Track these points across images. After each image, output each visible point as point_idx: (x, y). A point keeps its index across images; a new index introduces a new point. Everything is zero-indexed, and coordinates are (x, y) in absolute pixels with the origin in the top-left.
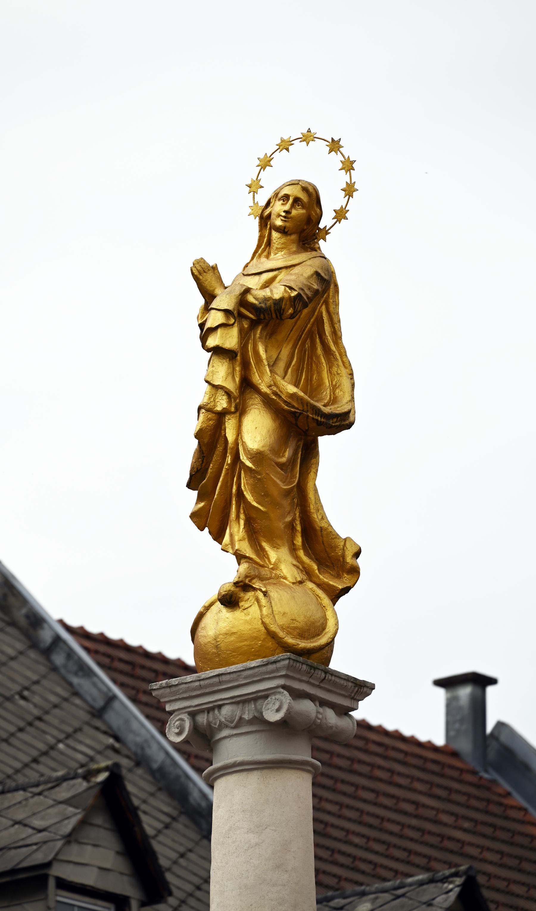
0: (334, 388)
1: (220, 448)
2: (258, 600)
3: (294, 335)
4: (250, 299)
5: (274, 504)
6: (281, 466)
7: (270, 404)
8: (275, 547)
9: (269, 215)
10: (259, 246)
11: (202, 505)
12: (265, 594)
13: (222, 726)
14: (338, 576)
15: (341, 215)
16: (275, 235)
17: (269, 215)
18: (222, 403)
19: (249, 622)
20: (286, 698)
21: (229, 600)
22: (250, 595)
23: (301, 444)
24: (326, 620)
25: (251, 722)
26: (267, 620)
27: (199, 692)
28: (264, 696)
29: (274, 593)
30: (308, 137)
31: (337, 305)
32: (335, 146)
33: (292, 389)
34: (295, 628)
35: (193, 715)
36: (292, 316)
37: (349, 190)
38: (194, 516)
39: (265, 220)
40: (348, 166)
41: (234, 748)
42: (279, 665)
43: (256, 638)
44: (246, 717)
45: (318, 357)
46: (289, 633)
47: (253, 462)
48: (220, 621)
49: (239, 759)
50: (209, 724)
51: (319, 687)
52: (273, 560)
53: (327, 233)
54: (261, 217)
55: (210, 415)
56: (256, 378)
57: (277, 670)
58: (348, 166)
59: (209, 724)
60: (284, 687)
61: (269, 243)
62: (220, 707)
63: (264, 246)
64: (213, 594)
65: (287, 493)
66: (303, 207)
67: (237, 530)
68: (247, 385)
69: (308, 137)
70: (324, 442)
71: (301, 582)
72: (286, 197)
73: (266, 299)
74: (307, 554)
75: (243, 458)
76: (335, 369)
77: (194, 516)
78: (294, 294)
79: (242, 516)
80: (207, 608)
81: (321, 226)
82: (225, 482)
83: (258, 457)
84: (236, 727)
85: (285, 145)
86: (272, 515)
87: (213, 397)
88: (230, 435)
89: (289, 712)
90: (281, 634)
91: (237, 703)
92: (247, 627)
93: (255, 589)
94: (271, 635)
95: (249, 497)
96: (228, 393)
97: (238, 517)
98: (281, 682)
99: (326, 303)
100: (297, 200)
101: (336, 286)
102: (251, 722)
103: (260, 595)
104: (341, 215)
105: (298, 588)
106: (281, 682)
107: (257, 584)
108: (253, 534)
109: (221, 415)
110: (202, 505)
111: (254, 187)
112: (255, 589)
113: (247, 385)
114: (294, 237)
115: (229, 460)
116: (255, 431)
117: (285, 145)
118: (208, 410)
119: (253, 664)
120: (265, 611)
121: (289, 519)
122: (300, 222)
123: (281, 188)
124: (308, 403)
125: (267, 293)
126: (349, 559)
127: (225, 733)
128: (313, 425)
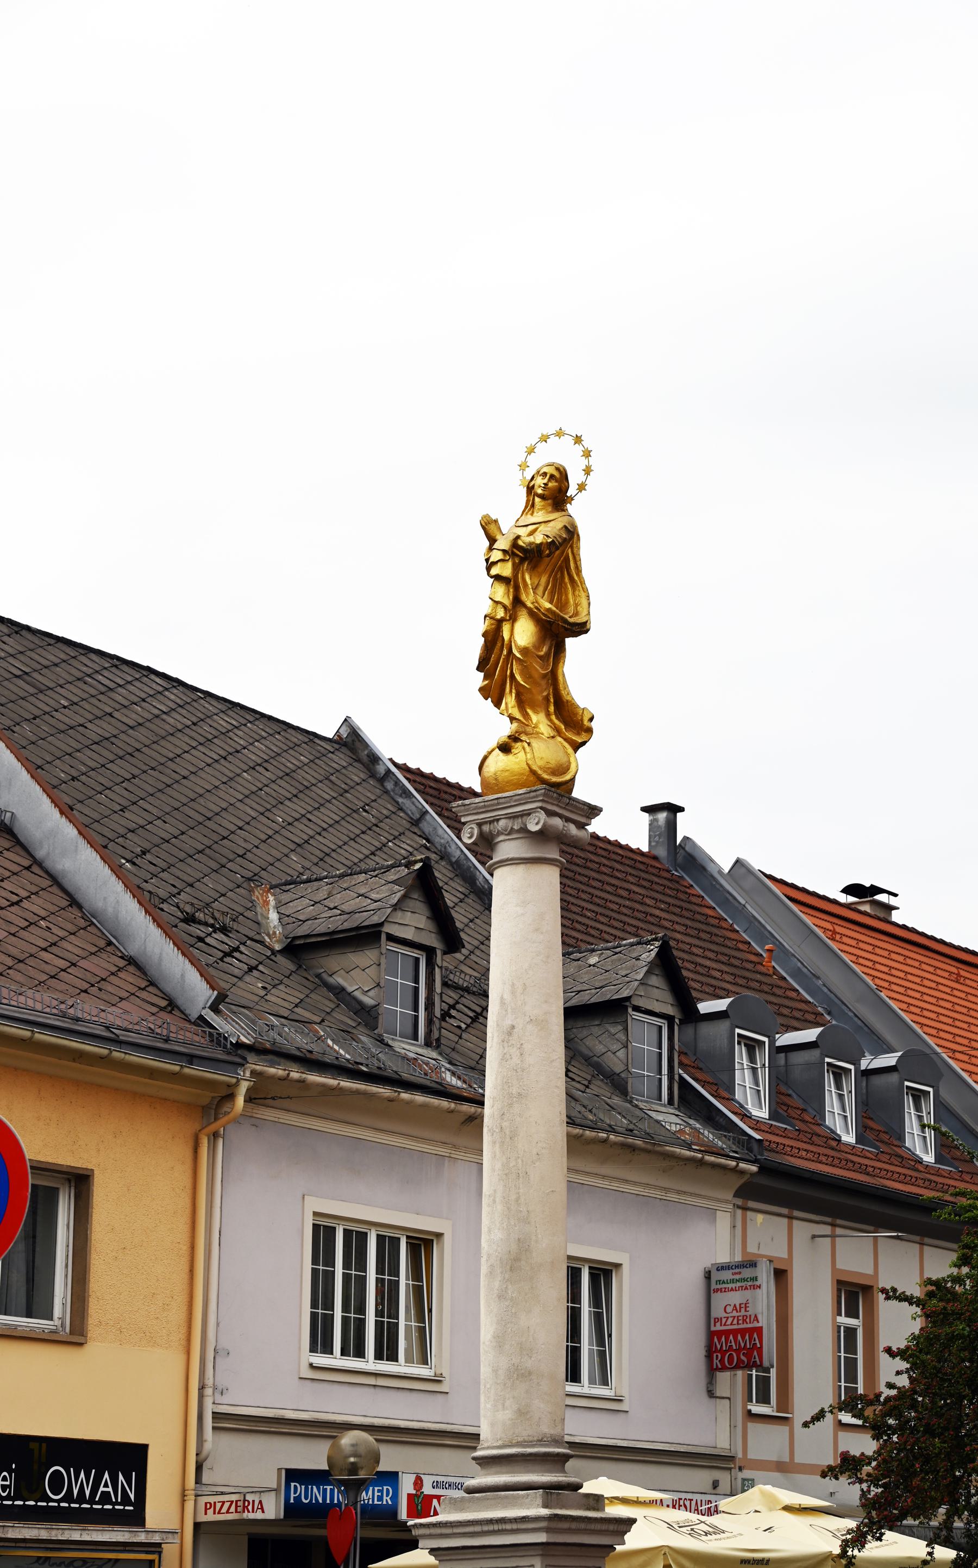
0: (576, 605)
1: (499, 644)
2: (524, 748)
3: (549, 568)
4: (520, 543)
5: (535, 683)
6: (540, 657)
7: (533, 614)
8: (536, 712)
9: (533, 486)
10: (526, 507)
11: (486, 682)
12: (529, 744)
13: (499, 833)
14: (578, 734)
15: (582, 487)
16: (537, 500)
17: (533, 486)
18: (500, 613)
19: (518, 763)
20: (542, 815)
21: (505, 748)
22: (519, 744)
23: (554, 643)
24: (570, 763)
25: (518, 831)
26: (530, 762)
28: (528, 813)
29: (535, 744)
30: (560, 433)
31: (579, 549)
32: (578, 440)
33: (548, 605)
34: (549, 768)
35: (480, 825)
36: (548, 556)
37: (588, 471)
38: (481, 690)
39: (530, 489)
40: (587, 454)
41: (507, 849)
42: (538, 793)
43: (522, 774)
44: (516, 827)
45: (566, 584)
46: (545, 771)
47: (521, 655)
48: (499, 762)
49: (511, 856)
50: (490, 831)
51: (564, 808)
52: (534, 721)
53: (572, 499)
54: (528, 487)
55: (493, 622)
56: (523, 597)
57: (537, 796)
58: (587, 454)
59: (490, 831)
60: (541, 808)
61: (533, 505)
62: (498, 820)
63: (530, 507)
64: (494, 744)
65: (544, 676)
66: (556, 481)
67: (510, 700)
68: (517, 602)
69: (560, 433)
70: (569, 642)
71: (553, 737)
72: (545, 474)
73: (531, 544)
74: (557, 718)
75: (515, 651)
76: (577, 593)
77: (481, 690)
78: (550, 540)
79: (514, 691)
80: (490, 753)
81: (568, 494)
82: (502, 668)
83: (524, 651)
84: (509, 834)
85: (544, 439)
86: (534, 691)
87: (494, 609)
88: (506, 635)
89: (544, 825)
90: (540, 772)
91: (510, 818)
92: (517, 767)
93: (522, 741)
94: (533, 772)
95: (518, 677)
96: (505, 607)
97: (511, 691)
98: (539, 804)
99: (572, 547)
100: (552, 476)
101: (578, 535)
102: (518, 831)
103: (526, 745)
104: (582, 487)
105: (551, 741)
106: (539, 804)
107: (523, 737)
108: (521, 703)
109: (500, 622)
110: (486, 682)
111: (523, 466)
112: (522, 741)
113: (517, 602)
114: (550, 501)
115: (505, 652)
116: (523, 633)
117: (544, 439)
118: (491, 618)
119: (521, 791)
120: (529, 756)
121: (545, 694)
122: (555, 492)
123: (541, 468)
124: (559, 615)
125: (531, 539)
126: (586, 722)
127: (501, 838)
128: (562, 630)
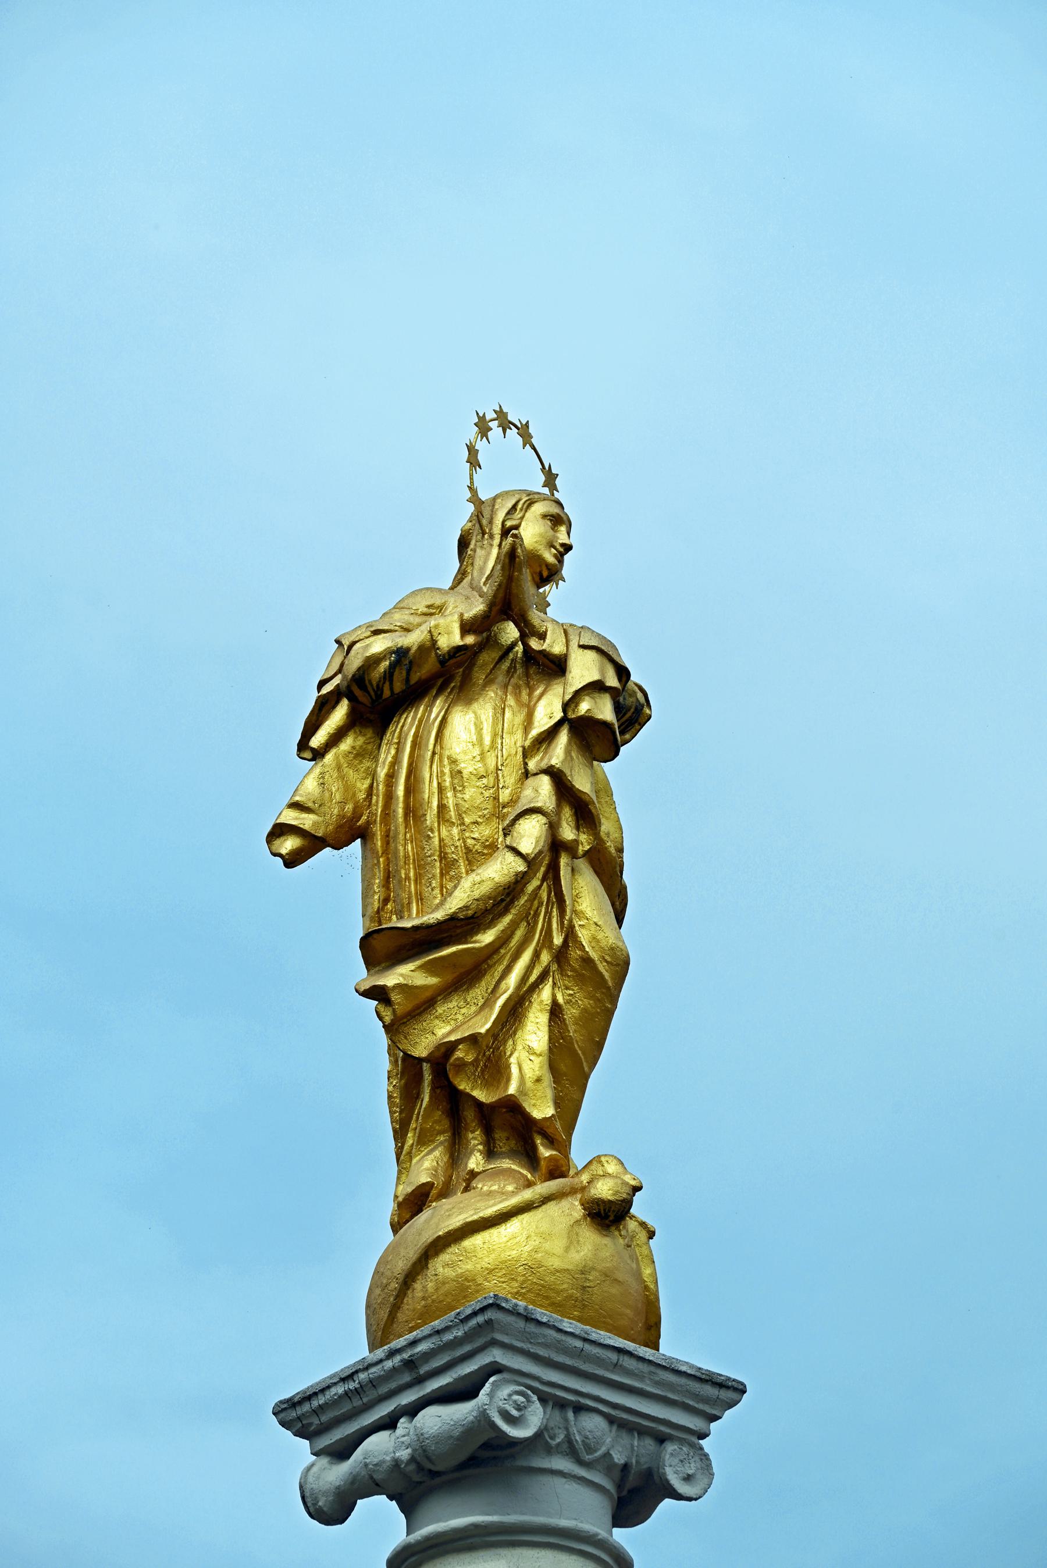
27: (568, 1361)
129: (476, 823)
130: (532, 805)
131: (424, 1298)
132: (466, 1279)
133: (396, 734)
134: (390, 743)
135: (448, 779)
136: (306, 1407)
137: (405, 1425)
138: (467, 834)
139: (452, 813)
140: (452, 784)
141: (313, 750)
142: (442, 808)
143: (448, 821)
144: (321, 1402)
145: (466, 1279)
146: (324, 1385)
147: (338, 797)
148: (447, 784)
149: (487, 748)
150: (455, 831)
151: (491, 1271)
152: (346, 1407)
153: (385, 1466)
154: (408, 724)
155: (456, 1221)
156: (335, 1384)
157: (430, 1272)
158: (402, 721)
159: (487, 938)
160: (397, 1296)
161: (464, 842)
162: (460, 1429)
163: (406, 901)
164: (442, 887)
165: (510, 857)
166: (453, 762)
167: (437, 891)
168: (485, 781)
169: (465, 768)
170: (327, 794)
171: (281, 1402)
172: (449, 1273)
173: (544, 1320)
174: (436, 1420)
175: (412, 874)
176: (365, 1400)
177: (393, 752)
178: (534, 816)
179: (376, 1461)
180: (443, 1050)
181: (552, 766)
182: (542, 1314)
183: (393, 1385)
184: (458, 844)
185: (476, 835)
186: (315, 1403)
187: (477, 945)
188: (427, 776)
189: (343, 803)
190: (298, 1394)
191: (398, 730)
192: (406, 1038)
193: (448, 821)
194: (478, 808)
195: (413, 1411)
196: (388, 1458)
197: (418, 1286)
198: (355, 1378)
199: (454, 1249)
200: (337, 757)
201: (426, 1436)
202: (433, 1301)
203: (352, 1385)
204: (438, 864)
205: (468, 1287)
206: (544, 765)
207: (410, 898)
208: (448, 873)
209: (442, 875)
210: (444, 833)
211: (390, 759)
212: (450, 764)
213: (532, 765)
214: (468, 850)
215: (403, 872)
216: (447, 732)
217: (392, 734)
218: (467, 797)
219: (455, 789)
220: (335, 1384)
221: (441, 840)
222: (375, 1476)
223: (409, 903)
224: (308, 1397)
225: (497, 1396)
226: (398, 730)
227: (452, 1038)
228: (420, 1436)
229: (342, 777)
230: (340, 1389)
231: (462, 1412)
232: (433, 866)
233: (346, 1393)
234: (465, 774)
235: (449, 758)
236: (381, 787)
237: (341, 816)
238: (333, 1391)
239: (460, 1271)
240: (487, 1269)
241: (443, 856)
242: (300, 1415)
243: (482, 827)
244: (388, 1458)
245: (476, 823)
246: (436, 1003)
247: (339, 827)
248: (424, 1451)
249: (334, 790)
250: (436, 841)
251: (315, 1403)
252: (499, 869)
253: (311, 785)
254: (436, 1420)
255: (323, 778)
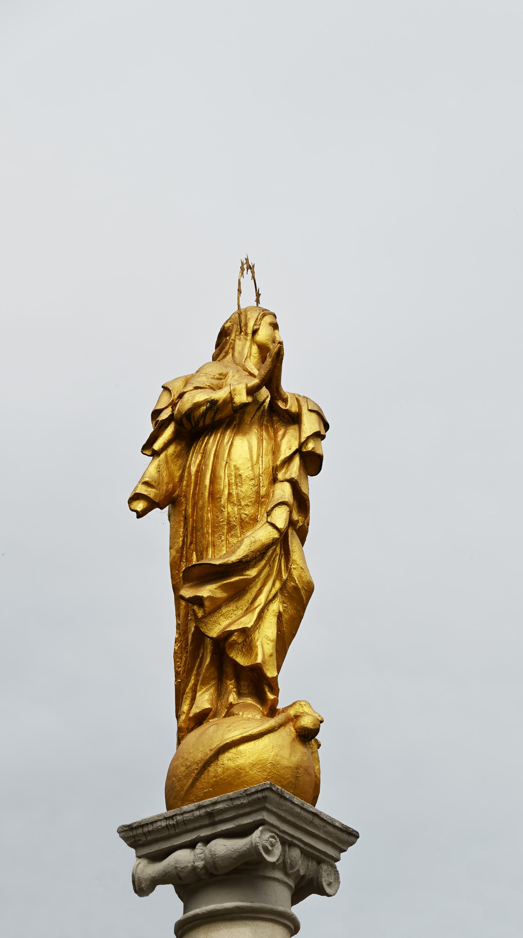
129: (247, 505)
130: (283, 500)
131: (215, 777)
132: (240, 768)
133: (202, 448)
134: (198, 453)
135: (233, 477)
136: (140, 831)
137: (201, 848)
138: (242, 511)
139: (235, 498)
140: (235, 481)
141: (154, 451)
142: (230, 494)
143: (232, 502)
144: (150, 829)
145: (240, 768)
146: (153, 820)
147: (166, 480)
148: (233, 481)
149: (255, 463)
150: (236, 509)
151: (254, 765)
152: (165, 833)
153: (187, 869)
154: (211, 443)
155: (235, 734)
156: (161, 820)
157: (220, 762)
158: (206, 440)
159: (252, 573)
160: (198, 774)
161: (240, 516)
162: (237, 854)
163: (205, 546)
164: (227, 540)
165: (270, 528)
166: (237, 469)
167: (224, 542)
168: (253, 482)
169: (243, 473)
170: (161, 478)
171: (124, 826)
172: (231, 764)
173: (288, 797)
174: (222, 847)
175: (210, 531)
176: (177, 831)
177: (200, 457)
178: (283, 506)
179: (183, 866)
180: (226, 635)
181: (293, 478)
182: (288, 794)
183: (197, 825)
184: (237, 516)
185: (247, 512)
186: (146, 829)
187: (249, 577)
188: (222, 474)
189: (168, 483)
190: (135, 823)
191: (203, 446)
192: (205, 625)
193: (232, 502)
194: (249, 497)
195: (207, 840)
196: (190, 865)
197: (212, 769)
198: (174, 818)
199: (233, 750)
200: (166, 456)
201: (217, 856)
202: (221, 779)
203: (171, 822)
204: (226, 527)
205: (241, 773)
206: (288, 477)
207: (208, 544)
208: (230, 532)
209: (227, 533)
210: (230, 509)
211: (198, 461)
212: (235, 470)
213: (280, 476)
214: (242, 521)
215: (206, 529)
216: (233, 450)
217: (199, 447)
218: (243, 490)
219: (237, 484)
220: (161, 820)
221: (228, 513)
222: (180, 874)
223: (207, 548)
224: (141, 825)
225: (259, 837)
226: (203, 446)
227: (233, 628)
228: (213, 856)
229: (168, 468)
230: (164, 824)
231: (238, 845)
232: (223, 528)
233: (167, 826)
234: (244, 476)
235: (235, 466)
236: (193, 478)
237: (167, 491)
238: (159, 824)
239: (237, 764)
240: (252, 764)
241: (229, 523)
242: (136, 836)
243: (250, 508)
244: (190, 865)
245: (247, 505)
246: (222, 606)
247: (166, 497)
248: (214, 864)
249: (164, 475)
250: (226, 513)
251: (146, 829)
252: (263, 534)
253: (152, 471)
254: (222, 847)
255: (159, 468)
